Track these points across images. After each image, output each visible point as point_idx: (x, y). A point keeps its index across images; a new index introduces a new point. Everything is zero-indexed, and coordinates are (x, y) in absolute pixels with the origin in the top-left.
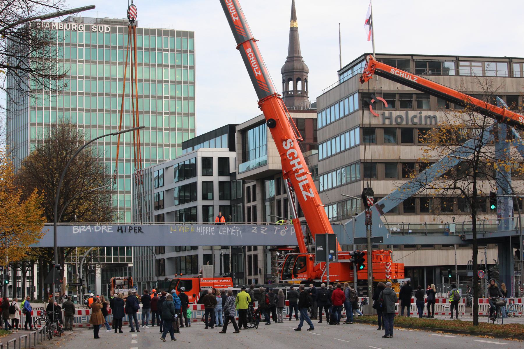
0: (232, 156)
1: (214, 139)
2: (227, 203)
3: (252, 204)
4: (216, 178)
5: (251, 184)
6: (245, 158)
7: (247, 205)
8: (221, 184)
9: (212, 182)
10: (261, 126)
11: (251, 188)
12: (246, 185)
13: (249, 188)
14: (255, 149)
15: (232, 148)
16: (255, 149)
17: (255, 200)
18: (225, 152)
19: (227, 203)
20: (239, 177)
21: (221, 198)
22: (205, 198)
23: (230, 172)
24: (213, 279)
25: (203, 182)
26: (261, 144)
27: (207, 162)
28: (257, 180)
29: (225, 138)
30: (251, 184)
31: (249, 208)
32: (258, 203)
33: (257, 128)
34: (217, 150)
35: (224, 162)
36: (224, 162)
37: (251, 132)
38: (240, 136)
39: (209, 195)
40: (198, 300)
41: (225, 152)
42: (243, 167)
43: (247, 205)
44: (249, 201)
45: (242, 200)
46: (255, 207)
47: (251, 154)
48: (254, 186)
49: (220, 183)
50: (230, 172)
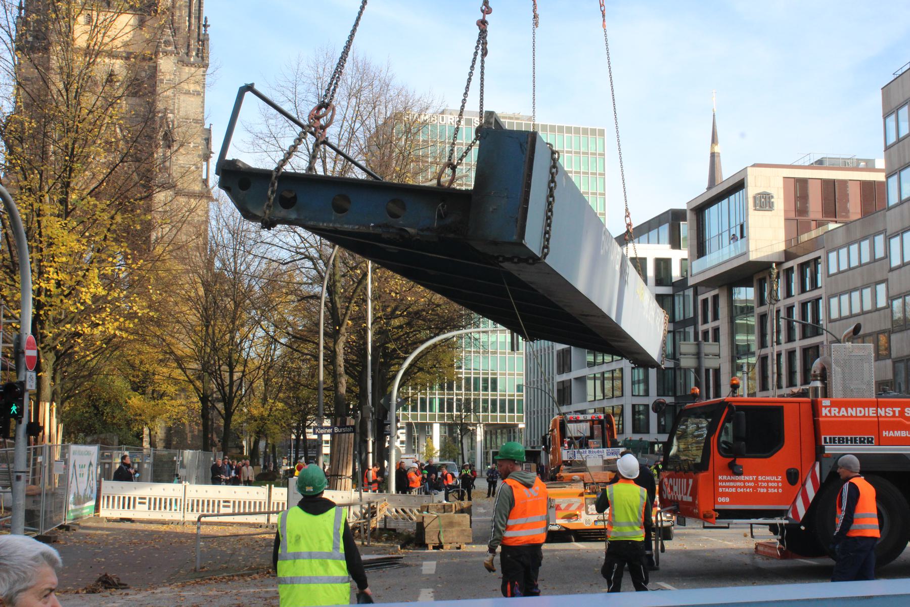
0: (676, 256)
1: (646, 235)
5: (709, 295)
6: (701, 250)
7: (701, 328)
10: (732, 197)
11: (710, 300)
12: (701, 298)
13: (705, 301)
14: (720, 235)
15: (675, 243)
16: (720, 235)
17: (716, 317)
18: (664, 250)
20: (691, 282)
24: (877, 405)
26: (733, 224)
28: (720, 287)
29: (665, 230)
30: (709, 295)
31: (706, 333)
33: (725, 202)
34: (652, 250)
35: (663, 265)
36: (663, 265)
37: (714, 209)
38: (694, 218)
40: (811, 494)
41: (664, 250)
42: (698, 266)
43: (701, 328)
45: (693, 321)
48: (716, 298)
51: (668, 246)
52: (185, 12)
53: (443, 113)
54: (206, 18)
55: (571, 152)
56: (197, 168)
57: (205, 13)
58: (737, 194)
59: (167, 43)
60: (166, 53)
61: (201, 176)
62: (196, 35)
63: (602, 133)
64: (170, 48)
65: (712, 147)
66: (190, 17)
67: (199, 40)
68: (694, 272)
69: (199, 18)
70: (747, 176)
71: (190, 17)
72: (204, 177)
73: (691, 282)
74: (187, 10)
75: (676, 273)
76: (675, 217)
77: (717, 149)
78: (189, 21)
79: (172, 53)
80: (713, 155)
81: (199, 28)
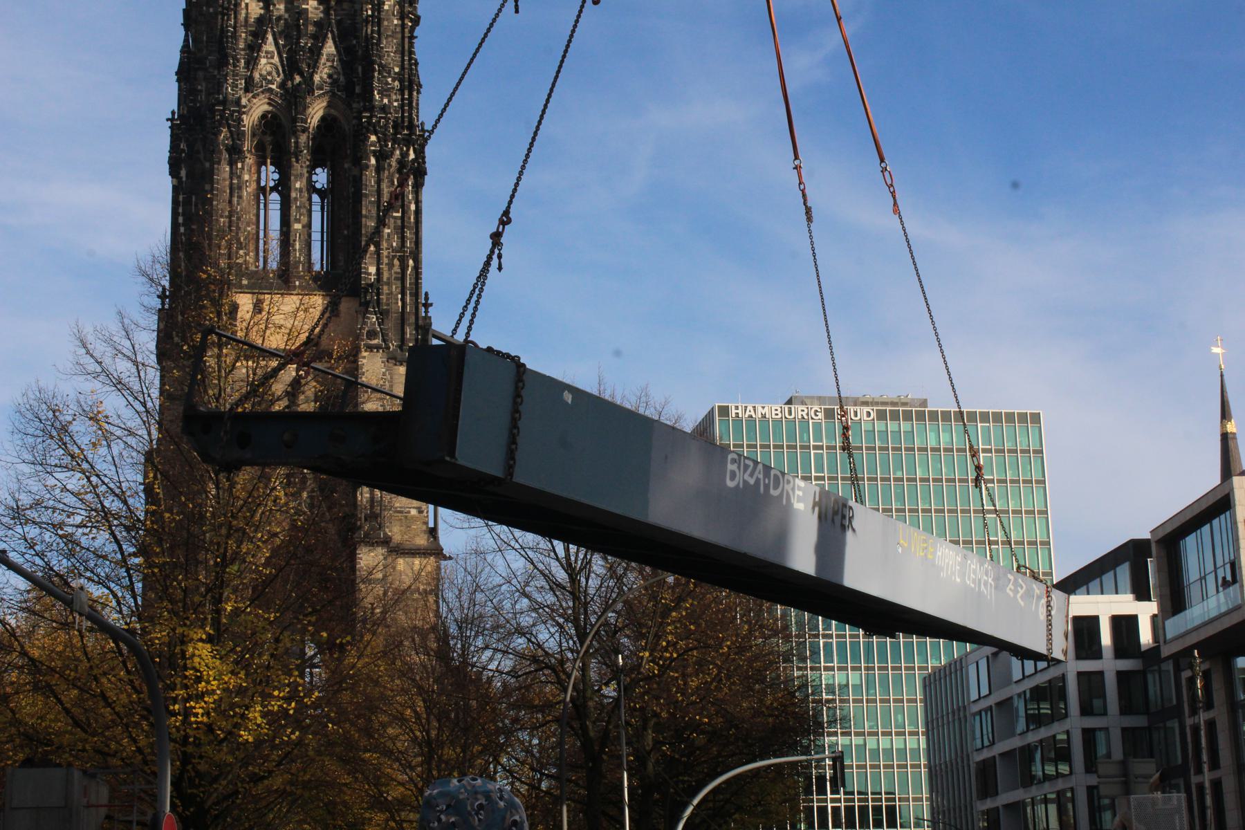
0: (1145, 612)
2: (1139, 721)
3: (1203, 717)
4: (1109, 665)
6: (1175, 601)
8: (1120, 674)
9: (1101, 673)
10: (1216, 522)
14: (1203, 578)
15: (1141, 594)
16: (1203, 578)
18: (1125, 604)
19: (1139, 721)
20: (1166, 651)
21: (1125, 710)
22: (1086, 711)
23: (1143, 649)
25: (1080, 674)
26: (1220, 563)
27: (1085, 629)
29: (1124, 571)
32: (1219, 713)
33: (1206, 528)
34: (1105, 605)
35: (1125, 626)
36: (1125, 626)
37: (1190, 542)
39: (1097, 703)
42: (1174, 626)
43: (1189, 722)
44: (1194, 712)
45: (1177, 712)
46: (1211, 724)
47: (1194, 592)
49: (1120, 674)
50: (1143, 649)
51: (1130, 597)
52: (395, 288)
53: (789, 402)
54: (426, 294)
55: (990, 451)
56: (420, 512)
57: (425, 286)
58: (1222, 517)
59: (372, 334)
60: (370, 348)
61: (426, 523)
62: (412, 320)
63: (1036, 418)
64: (376, 342)
65: (1223, 426)
66: (403, 293)
67: (417, 327)
68: (1169, 636)
69: (416, 294)
70: (1232, 489)
71: (403, 293)
72: (431, 525)
73: (1166, 651)
74: (399, 284)
75: (1146, 636)
76: (1133, 552)
77: (1231, 427)
78: (403, 300)
79: (378, 347)
80: (1226, 438)
81: (417, 309)
